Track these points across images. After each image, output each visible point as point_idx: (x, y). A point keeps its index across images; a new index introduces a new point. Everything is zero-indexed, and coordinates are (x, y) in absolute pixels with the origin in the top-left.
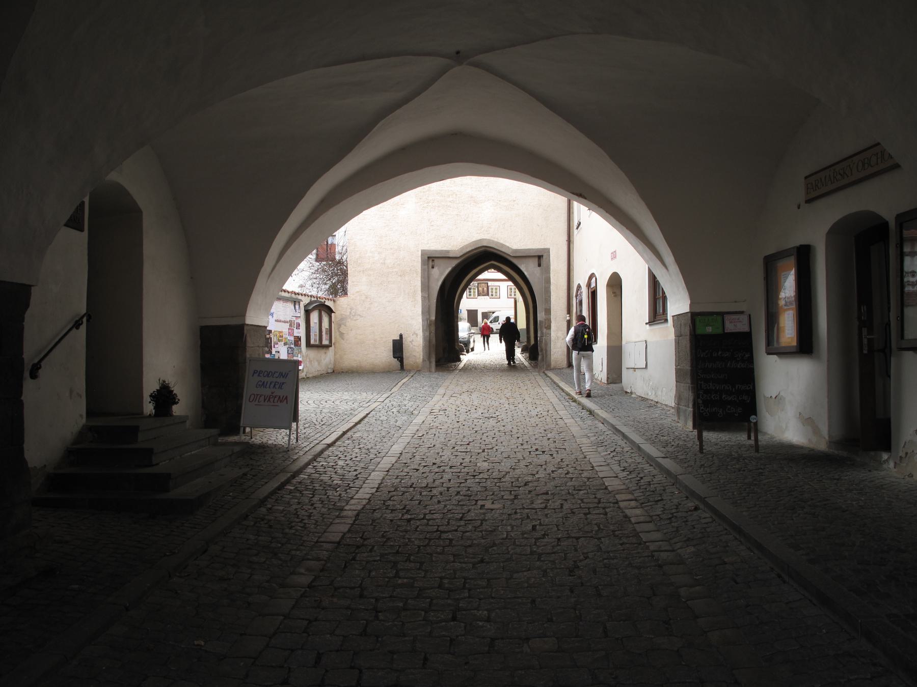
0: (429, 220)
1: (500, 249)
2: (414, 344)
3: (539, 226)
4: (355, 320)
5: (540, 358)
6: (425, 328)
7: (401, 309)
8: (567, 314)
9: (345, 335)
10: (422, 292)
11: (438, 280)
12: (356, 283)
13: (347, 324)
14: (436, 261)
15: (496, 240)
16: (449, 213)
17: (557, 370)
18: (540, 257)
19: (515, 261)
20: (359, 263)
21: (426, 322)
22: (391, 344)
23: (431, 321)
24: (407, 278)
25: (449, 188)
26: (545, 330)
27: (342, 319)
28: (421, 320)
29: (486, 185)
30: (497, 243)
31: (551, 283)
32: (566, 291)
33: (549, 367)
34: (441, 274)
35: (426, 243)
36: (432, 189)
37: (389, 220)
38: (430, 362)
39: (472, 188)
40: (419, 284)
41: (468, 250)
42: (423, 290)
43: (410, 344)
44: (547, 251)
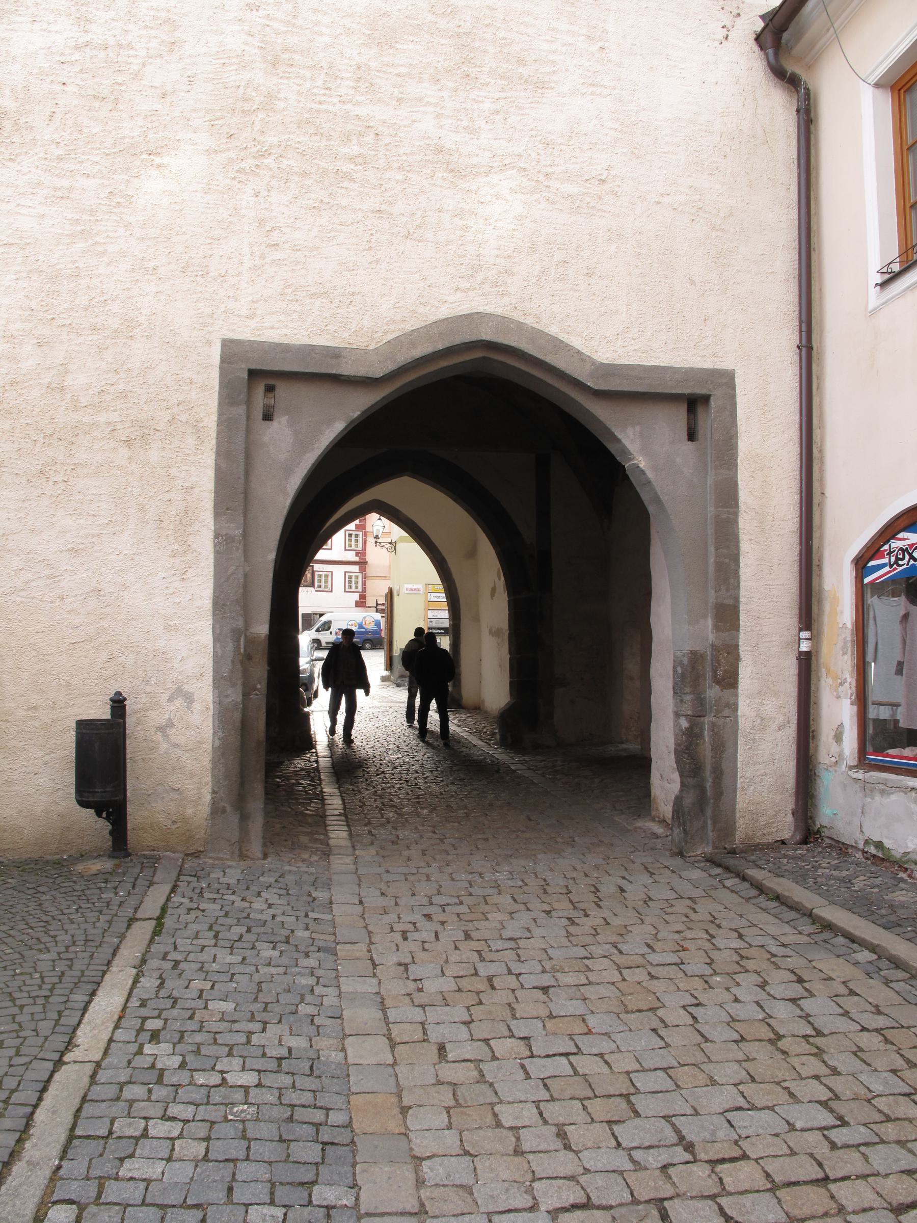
0: (261, 222)
1: (549, 359)
3: (692, 282)
6: (225, 671)
7: (125, 587)
8: (800, 630)
10: (217, 515)
11: (288, 472)
14: (283, 390)
15: (530, 321)
16: (344, 202)
18: (705, 399)
19: (601, 412)
21: (230, 647)
22: (70, 739)
23: (251, 641)
24: (154, 455)
25: (348, 106)
28: (207, 638)
29: (498, 112)
30: (537, 335)
31: (742, 507)
34: (302, 446)
36: (281, 105)
37: (92, 212)
38: (244, 817)
42: (221, 508)
43: (159, 738)
44: (726, 379)
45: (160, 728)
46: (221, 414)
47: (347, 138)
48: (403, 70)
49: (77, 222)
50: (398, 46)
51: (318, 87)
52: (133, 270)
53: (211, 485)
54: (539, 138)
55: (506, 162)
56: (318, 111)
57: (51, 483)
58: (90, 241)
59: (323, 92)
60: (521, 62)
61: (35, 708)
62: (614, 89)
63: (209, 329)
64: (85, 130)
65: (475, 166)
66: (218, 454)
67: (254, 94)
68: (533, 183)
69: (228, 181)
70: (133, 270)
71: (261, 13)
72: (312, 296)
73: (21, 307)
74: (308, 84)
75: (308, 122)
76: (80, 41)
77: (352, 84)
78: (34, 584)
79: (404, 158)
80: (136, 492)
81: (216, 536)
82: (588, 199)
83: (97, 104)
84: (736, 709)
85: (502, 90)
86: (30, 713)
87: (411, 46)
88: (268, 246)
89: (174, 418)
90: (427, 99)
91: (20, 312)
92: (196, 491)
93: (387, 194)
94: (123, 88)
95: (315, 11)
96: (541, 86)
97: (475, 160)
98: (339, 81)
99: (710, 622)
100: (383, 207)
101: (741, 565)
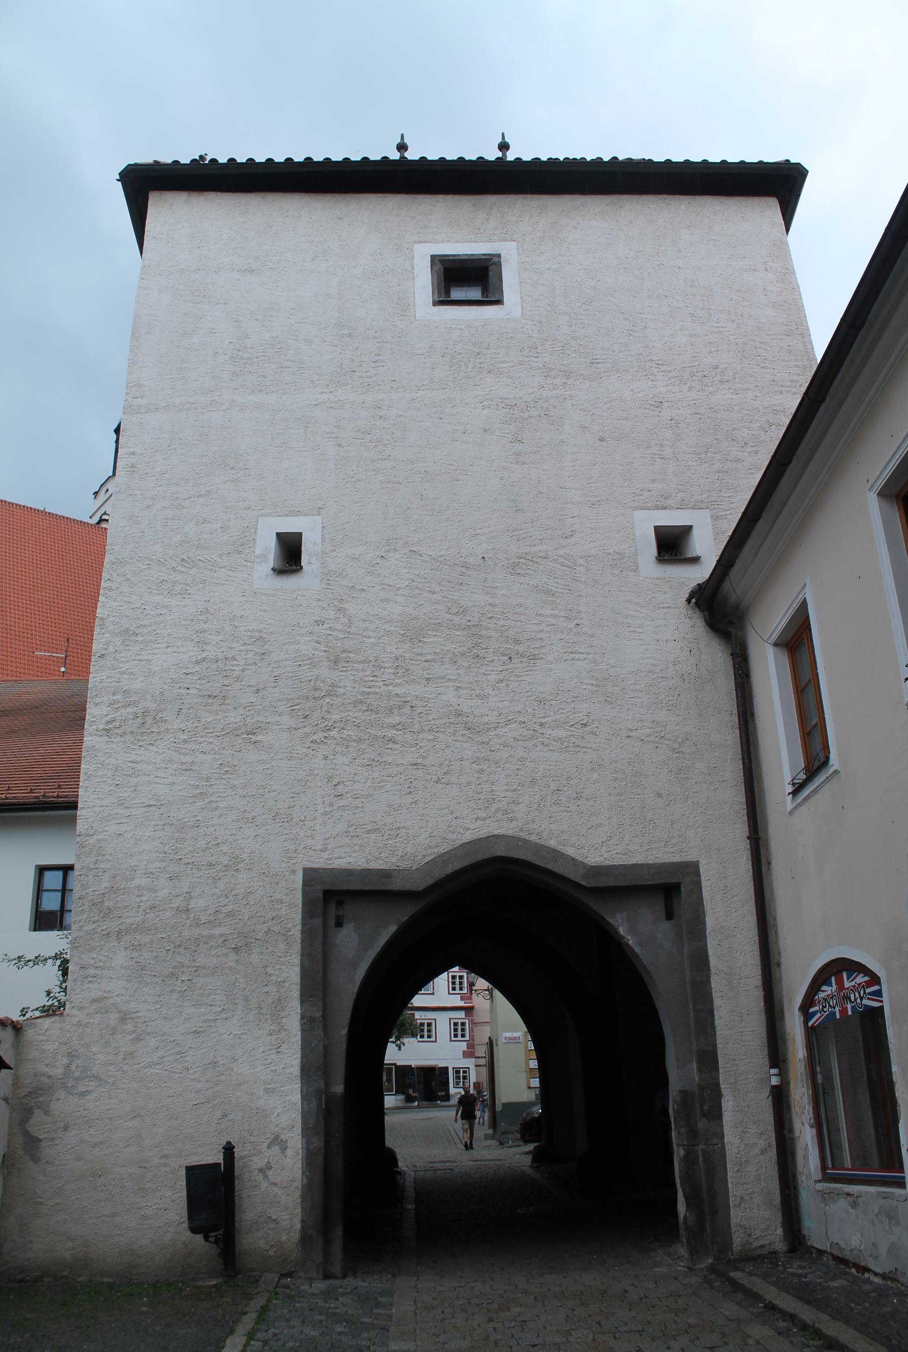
0: (330, 779)
1: (549, 867)
2: (272, 1179)
3: (660, 795)
4: (83, 1094)
8: (771, 1067)
9: (44, 1144)
10: (303, 1001)
12: (92, 971)
13: (55, 1107)
16: (390, 759)
21: (314, 1104)
23: (330, 1098)
24: (255, 958)
25: (390, 688)
28: (297, 1097)
30: (540, 848)
31: (713, 970)
32: (759, 993)
36: (342, 691)
37: (208, 779)
38: (327, 1243)
40: (292, 974)
41: (449, 869)
44: (692, 869)
45: (261, 1170)
46: (304, 924)
48: (429, 657)
51: (368, 676)
52: (238, 820)
53: (298, 979)
54: (533, 698)
55: (510, 718)
56: (368, 693)
57: (179, 982)
58: (207, 801)
60: (517, 642)
61: (166, 1156)
63: (294, 861)
64: (203, 720)
66: (302, 955)
67: (322, 685)
69: (305, 750)
70: (238, 820)
72: (369, 832)
73: (157, 851)
74: (360, 674)
75: (361, 702)
76: (199, 657)
77: (392, 671)
78: (166, 1059)
80: (242, 986)
81: (302, 1018)
82: (573, 740)
83: (210, 701)
84: (723, 1137)
86: (163, 1161)
88: (336, 796)
89: (269, 930)
90: (448, 677)
91: (157, 855)
92: (286, 984)
93: (421, 751)
94: (229, 688)
95: (364, 620)
96: (533, 658)
97: (486, 719)
98: (383, 670)
99: (695, 1065)
100: (419, 761)
101: (716, 1018)
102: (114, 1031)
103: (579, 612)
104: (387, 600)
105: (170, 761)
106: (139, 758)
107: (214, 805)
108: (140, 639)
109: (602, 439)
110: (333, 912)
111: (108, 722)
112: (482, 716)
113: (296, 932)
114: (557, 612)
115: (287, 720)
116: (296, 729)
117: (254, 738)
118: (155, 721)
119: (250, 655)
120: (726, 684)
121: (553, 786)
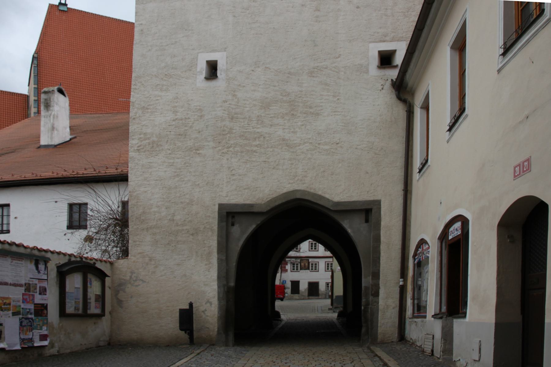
4: (137, 286)
5: (363, 330)
12: (138, 243)
16: (254, 159)
17: (383, 344)
20: (143, 219)
25: (255, 129)
26: (371, 298)
27: (120, 285)
29: (303, 125)
33: (374, 341)
35: (224, 196)
36: (234, 131)
39: (284, 129)
47: (255, 139)
48: (272, 115)
49: (175, 172)
50: (271, 108)
51: (246, 124)
52: (192, 185)
54: (316, 132)
55: (305, 141)
56: (246, 132)
57: (171, 246)
58: (180, 178)
59: (247, 126)
60: (311, 108)
62: (342, 112)
63: (214, 201)
64: (177, 145)
65: (295, 144)
66: (218, 236)
67: (226, 129)
68: (314, 147)
69: (219, 156)
70: (192, 185)
71: (228, 103)
72: (245, 189)
73: (161, 198)
74: (243, 124)
76: (175, 118)
77: (256, 122)
79: (273, 144)
82: (332, 150)
83: (180, 137)
85: (305, 118)
87: (275, 107)
88: (232, 175)
89: (205, 227)
90: (281, 124)
91: (161, 199)
92: (212, 247)
93: (268, 156)
94: (187, 131)
95: (244, 100)
96: (318, 114)
97: (295, 142)
98: (252, 122)
100: (266, 160)
102: (147, 264)
103: (339, 93)
104: (254, 91)
105: (164, 162)
106: (152, 161)
107: (183, 179)
108: (149, 111)
109: (358, 7)
110: (230, 220)
111: (138, 147)
112: (294, 140)
113: (216, 228)
114: (329, 94)
115: (211, 144)
116: (215, 148)
117: (198, 152)
118: (158, 146)
119: (196, 117)
120: (403, 124)
121: (322, 170)
